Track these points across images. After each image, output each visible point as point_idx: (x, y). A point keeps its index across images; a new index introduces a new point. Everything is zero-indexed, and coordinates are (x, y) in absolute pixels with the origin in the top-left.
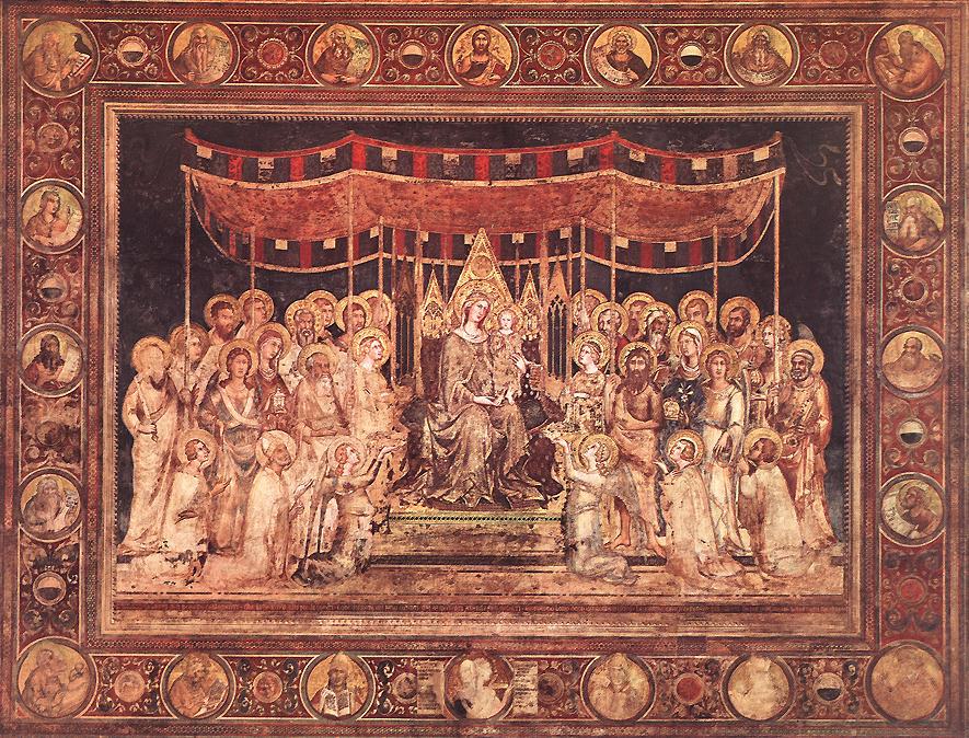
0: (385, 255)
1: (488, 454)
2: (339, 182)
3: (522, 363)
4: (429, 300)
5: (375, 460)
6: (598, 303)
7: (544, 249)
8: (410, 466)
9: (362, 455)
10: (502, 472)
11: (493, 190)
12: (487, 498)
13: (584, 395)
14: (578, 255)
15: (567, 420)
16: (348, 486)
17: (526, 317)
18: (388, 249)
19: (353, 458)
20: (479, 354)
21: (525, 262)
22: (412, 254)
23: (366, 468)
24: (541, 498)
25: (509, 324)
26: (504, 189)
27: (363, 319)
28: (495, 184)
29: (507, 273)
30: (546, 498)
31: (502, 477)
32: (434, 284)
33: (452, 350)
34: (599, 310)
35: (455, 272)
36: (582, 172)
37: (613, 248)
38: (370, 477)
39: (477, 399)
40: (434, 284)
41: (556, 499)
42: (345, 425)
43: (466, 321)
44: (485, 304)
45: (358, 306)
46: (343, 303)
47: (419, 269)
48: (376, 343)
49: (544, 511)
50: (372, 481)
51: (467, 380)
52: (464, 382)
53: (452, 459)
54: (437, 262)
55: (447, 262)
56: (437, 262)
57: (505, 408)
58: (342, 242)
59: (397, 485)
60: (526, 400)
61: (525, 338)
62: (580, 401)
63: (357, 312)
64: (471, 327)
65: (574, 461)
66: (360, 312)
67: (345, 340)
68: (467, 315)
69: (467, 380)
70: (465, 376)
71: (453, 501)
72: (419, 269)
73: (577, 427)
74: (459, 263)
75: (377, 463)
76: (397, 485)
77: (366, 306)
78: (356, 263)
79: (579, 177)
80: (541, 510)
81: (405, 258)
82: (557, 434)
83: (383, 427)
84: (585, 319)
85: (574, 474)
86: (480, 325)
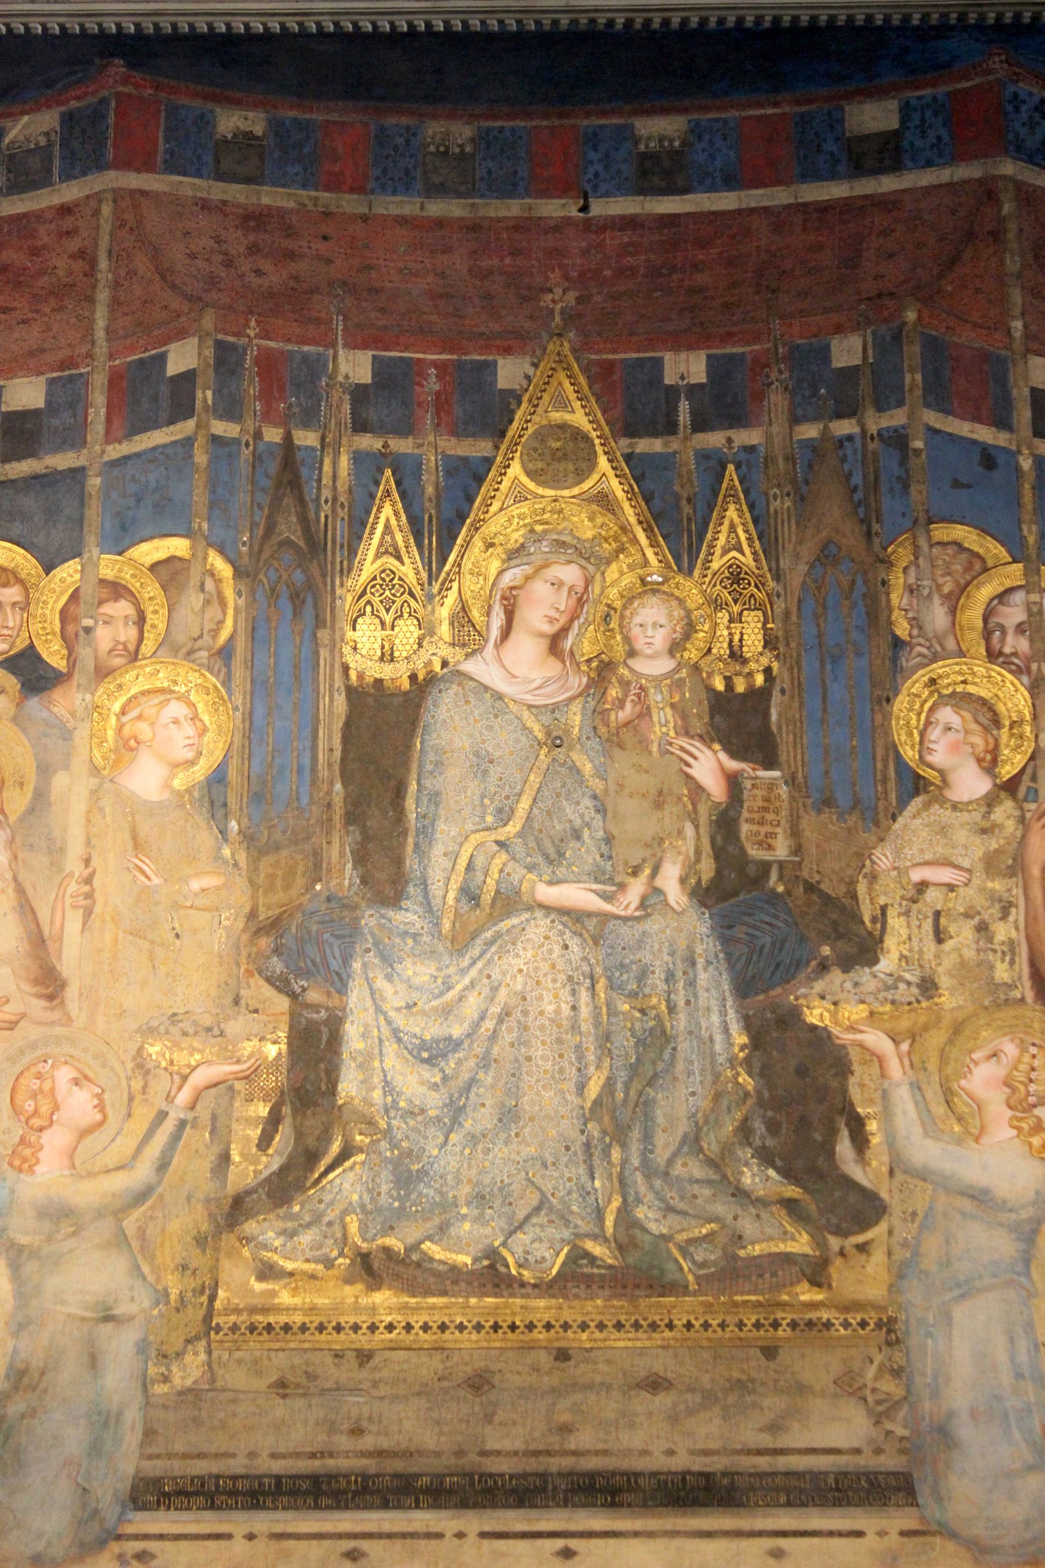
0: (220, 428)
1: (593, 1090)
2: (65, 210)
3: (709, 766)
4: (370, 563)
5: (162, 1116)
6: (979, 567)
7: (778, 400)
8: (299, 1135)
9: (115, 1102)
10: (647, 1151)
11: (589, 226)
12: (597, 1249)
13: (945, 875)
14: (896, 418)
15: (886, 964)
16: (59, 1215)
17: (723, 617)
18: (230, 410)
19: (79, 1105)
20: (556, 742)
21: (715, 439)
22: (309, 418)
23: (126, 1144)
24: (801, 1244)
25: (660, 639)
26: (629, 223)
27: (132, 632)
28: (599, 208)
29: (641, 472)
30: (820, 1243)
31: (648, 1170)
32: (388, 514)
33: (451, 726)
34: (985, 592)
35: (468, 480)
36: (896, 167)
37: (1021, 395)
38: (143, 1172)
39: (545, 893)
40: (388, 514)
41: (862, 1248)
42: (50, 984)
43: (506, 632)
44: (570, 574)
45: (116, 590)
46: (69, 572)
47: (340, 468)
48: (176, 709)
49: (819, 1296)
50: (142, 1196)
51: (513, 828)
52: (502, 834)
53: (456, 1112)
54: (401, 446)
55: (432, 448)
56: (401, 446)
57: (653, 925)
58: (68, 395)
59: (237, 1209)
60: (732, 888)
61: (719, 685)
62: (932, 895)
63: (110, 609)
64: (525, 653)
65: (923, 1106)
66: (122, 608)
67: (65, 702)
68: (510, 615)
69: (513, 828)
70: (504, 816)
71: (464, 1259)
72: (340, 468)
73: (928, 986)
74: (478, 448)
75: (168, 1126)
76: (237, 1209)
77: (151, 590)
78: (116, 451)
79: (888, 184)
80: (807, 1294)
81: (288, 438)
82: (854, 1012)
83: (196, 989)
84: (938, 616)
85: (925, 1151)
86: (554, 644)
